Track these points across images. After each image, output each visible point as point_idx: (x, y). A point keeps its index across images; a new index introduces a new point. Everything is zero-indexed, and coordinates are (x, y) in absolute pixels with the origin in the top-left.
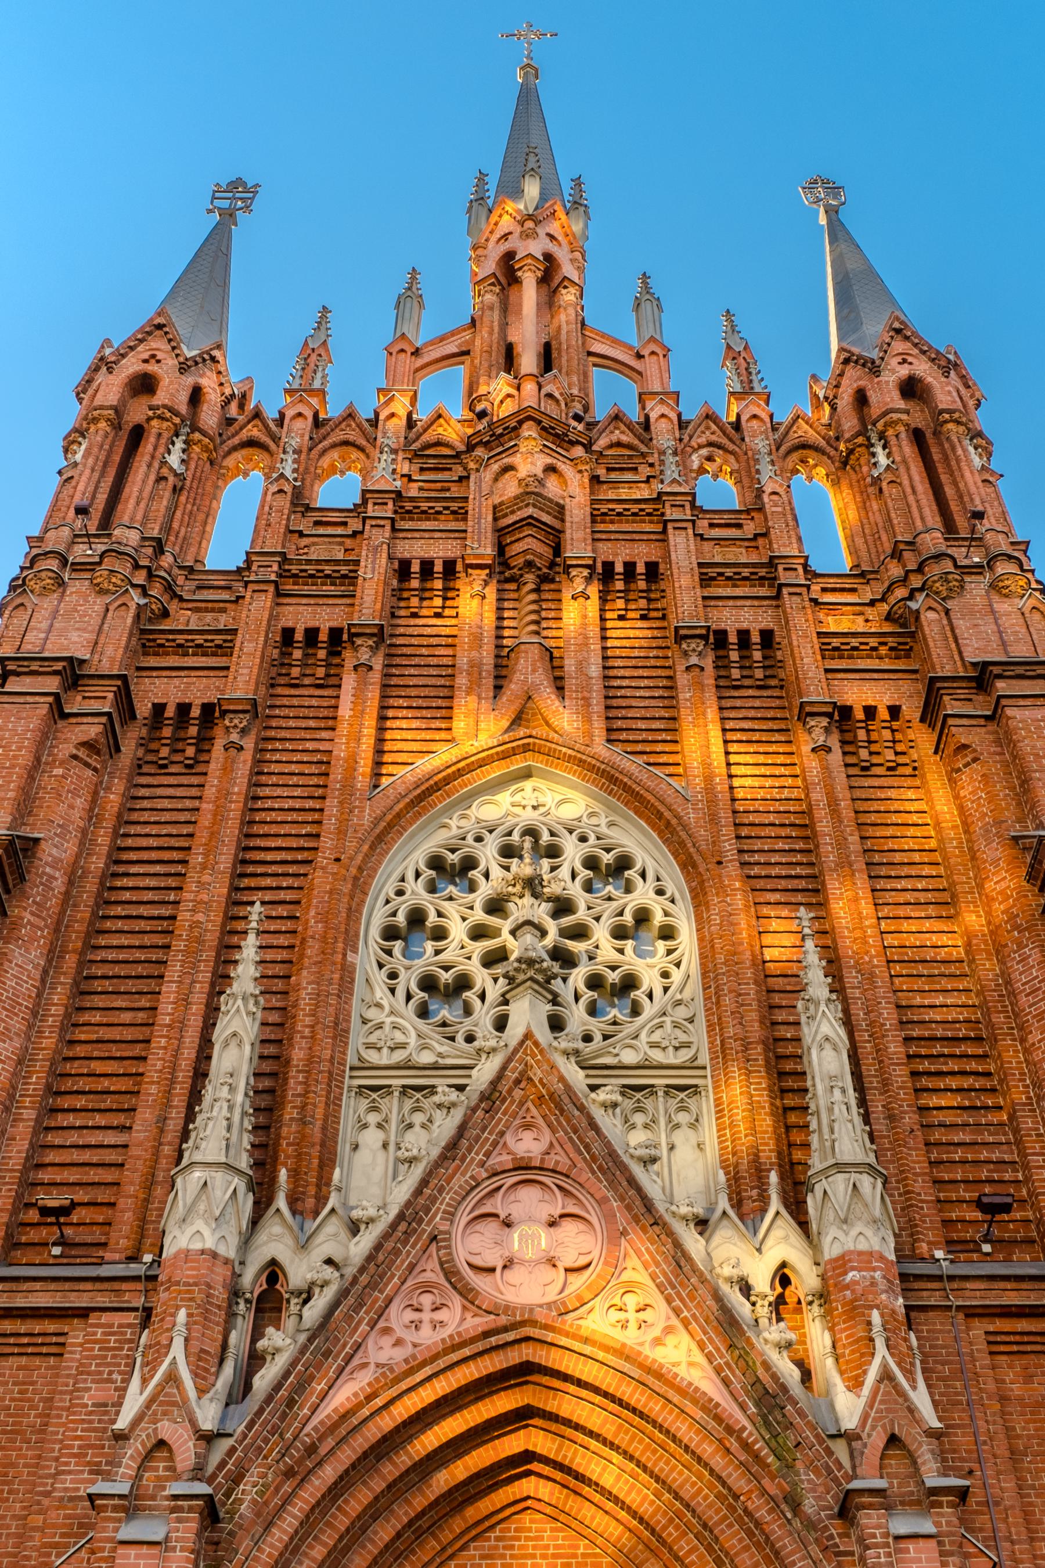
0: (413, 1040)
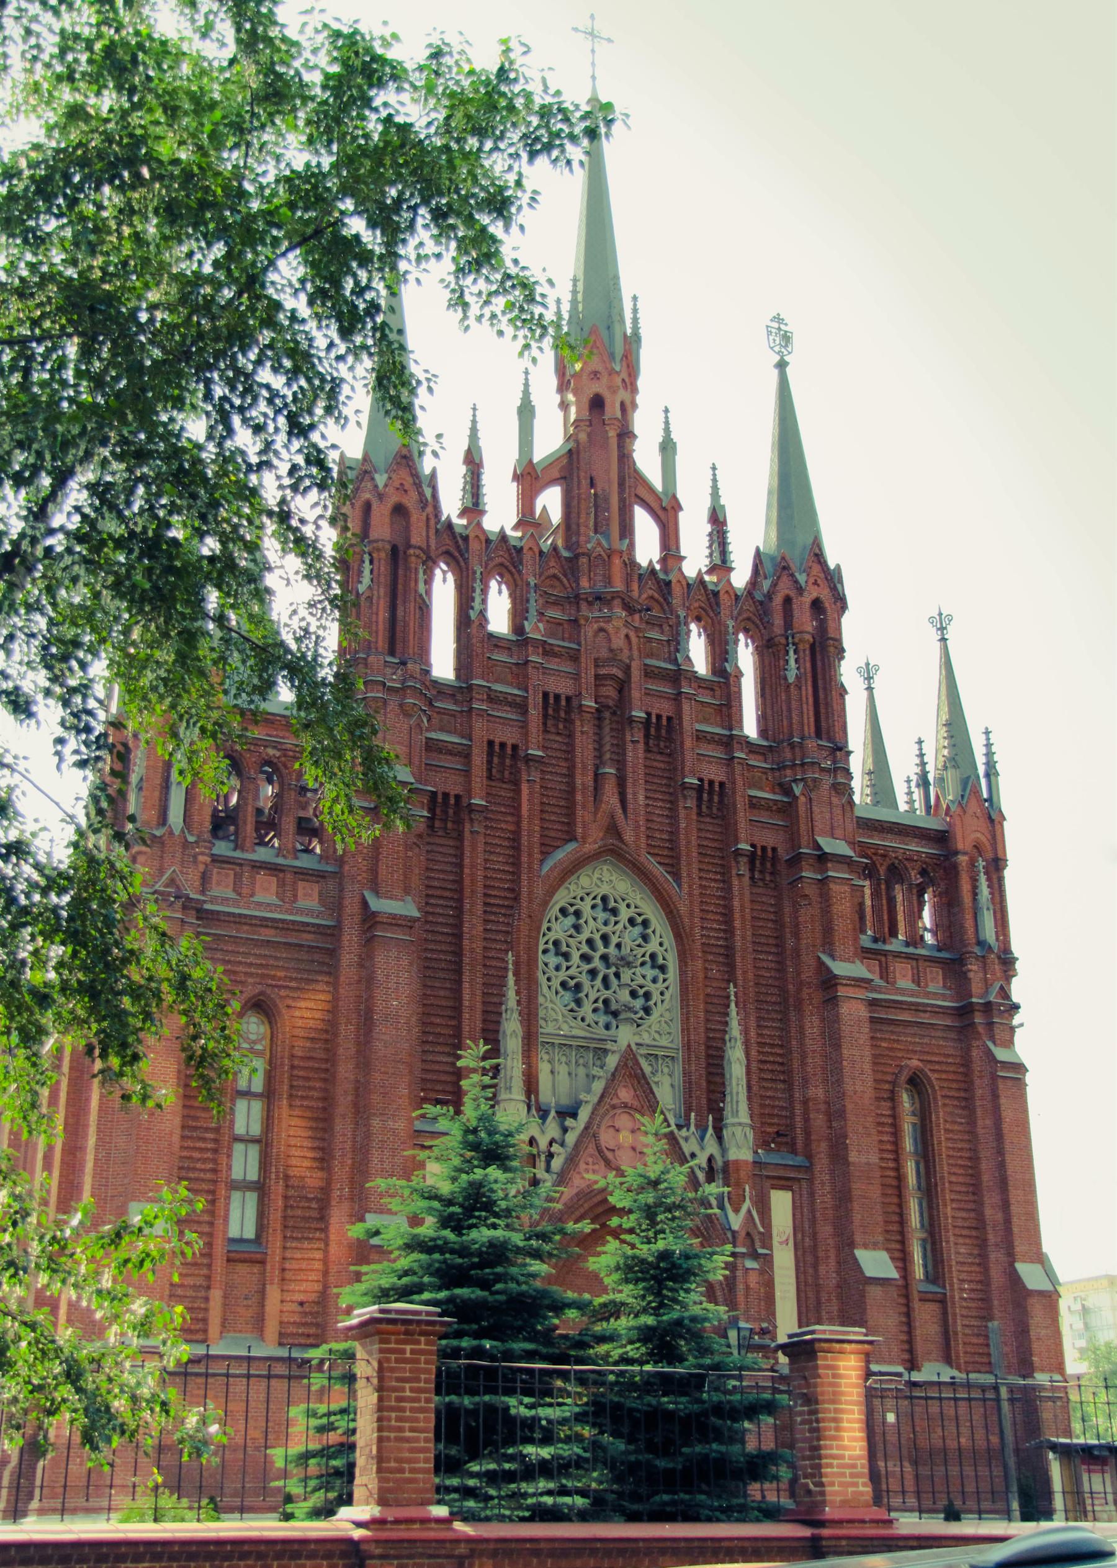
0: (560, 1018)
